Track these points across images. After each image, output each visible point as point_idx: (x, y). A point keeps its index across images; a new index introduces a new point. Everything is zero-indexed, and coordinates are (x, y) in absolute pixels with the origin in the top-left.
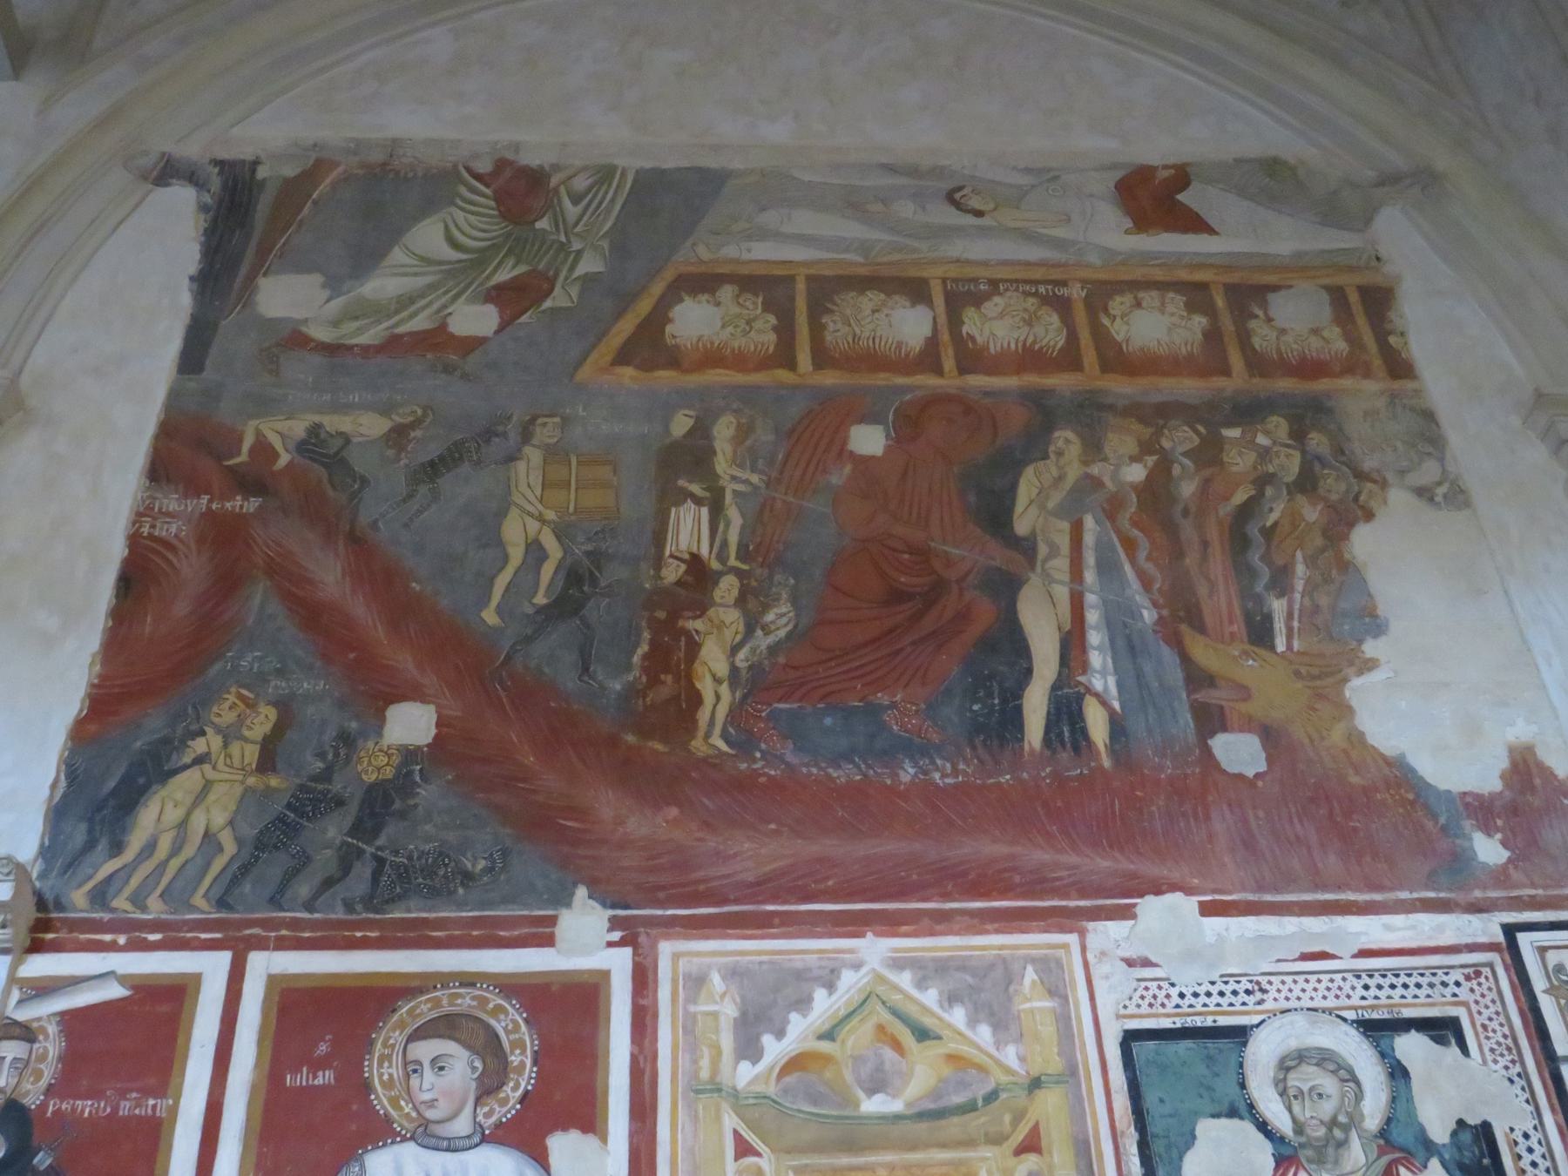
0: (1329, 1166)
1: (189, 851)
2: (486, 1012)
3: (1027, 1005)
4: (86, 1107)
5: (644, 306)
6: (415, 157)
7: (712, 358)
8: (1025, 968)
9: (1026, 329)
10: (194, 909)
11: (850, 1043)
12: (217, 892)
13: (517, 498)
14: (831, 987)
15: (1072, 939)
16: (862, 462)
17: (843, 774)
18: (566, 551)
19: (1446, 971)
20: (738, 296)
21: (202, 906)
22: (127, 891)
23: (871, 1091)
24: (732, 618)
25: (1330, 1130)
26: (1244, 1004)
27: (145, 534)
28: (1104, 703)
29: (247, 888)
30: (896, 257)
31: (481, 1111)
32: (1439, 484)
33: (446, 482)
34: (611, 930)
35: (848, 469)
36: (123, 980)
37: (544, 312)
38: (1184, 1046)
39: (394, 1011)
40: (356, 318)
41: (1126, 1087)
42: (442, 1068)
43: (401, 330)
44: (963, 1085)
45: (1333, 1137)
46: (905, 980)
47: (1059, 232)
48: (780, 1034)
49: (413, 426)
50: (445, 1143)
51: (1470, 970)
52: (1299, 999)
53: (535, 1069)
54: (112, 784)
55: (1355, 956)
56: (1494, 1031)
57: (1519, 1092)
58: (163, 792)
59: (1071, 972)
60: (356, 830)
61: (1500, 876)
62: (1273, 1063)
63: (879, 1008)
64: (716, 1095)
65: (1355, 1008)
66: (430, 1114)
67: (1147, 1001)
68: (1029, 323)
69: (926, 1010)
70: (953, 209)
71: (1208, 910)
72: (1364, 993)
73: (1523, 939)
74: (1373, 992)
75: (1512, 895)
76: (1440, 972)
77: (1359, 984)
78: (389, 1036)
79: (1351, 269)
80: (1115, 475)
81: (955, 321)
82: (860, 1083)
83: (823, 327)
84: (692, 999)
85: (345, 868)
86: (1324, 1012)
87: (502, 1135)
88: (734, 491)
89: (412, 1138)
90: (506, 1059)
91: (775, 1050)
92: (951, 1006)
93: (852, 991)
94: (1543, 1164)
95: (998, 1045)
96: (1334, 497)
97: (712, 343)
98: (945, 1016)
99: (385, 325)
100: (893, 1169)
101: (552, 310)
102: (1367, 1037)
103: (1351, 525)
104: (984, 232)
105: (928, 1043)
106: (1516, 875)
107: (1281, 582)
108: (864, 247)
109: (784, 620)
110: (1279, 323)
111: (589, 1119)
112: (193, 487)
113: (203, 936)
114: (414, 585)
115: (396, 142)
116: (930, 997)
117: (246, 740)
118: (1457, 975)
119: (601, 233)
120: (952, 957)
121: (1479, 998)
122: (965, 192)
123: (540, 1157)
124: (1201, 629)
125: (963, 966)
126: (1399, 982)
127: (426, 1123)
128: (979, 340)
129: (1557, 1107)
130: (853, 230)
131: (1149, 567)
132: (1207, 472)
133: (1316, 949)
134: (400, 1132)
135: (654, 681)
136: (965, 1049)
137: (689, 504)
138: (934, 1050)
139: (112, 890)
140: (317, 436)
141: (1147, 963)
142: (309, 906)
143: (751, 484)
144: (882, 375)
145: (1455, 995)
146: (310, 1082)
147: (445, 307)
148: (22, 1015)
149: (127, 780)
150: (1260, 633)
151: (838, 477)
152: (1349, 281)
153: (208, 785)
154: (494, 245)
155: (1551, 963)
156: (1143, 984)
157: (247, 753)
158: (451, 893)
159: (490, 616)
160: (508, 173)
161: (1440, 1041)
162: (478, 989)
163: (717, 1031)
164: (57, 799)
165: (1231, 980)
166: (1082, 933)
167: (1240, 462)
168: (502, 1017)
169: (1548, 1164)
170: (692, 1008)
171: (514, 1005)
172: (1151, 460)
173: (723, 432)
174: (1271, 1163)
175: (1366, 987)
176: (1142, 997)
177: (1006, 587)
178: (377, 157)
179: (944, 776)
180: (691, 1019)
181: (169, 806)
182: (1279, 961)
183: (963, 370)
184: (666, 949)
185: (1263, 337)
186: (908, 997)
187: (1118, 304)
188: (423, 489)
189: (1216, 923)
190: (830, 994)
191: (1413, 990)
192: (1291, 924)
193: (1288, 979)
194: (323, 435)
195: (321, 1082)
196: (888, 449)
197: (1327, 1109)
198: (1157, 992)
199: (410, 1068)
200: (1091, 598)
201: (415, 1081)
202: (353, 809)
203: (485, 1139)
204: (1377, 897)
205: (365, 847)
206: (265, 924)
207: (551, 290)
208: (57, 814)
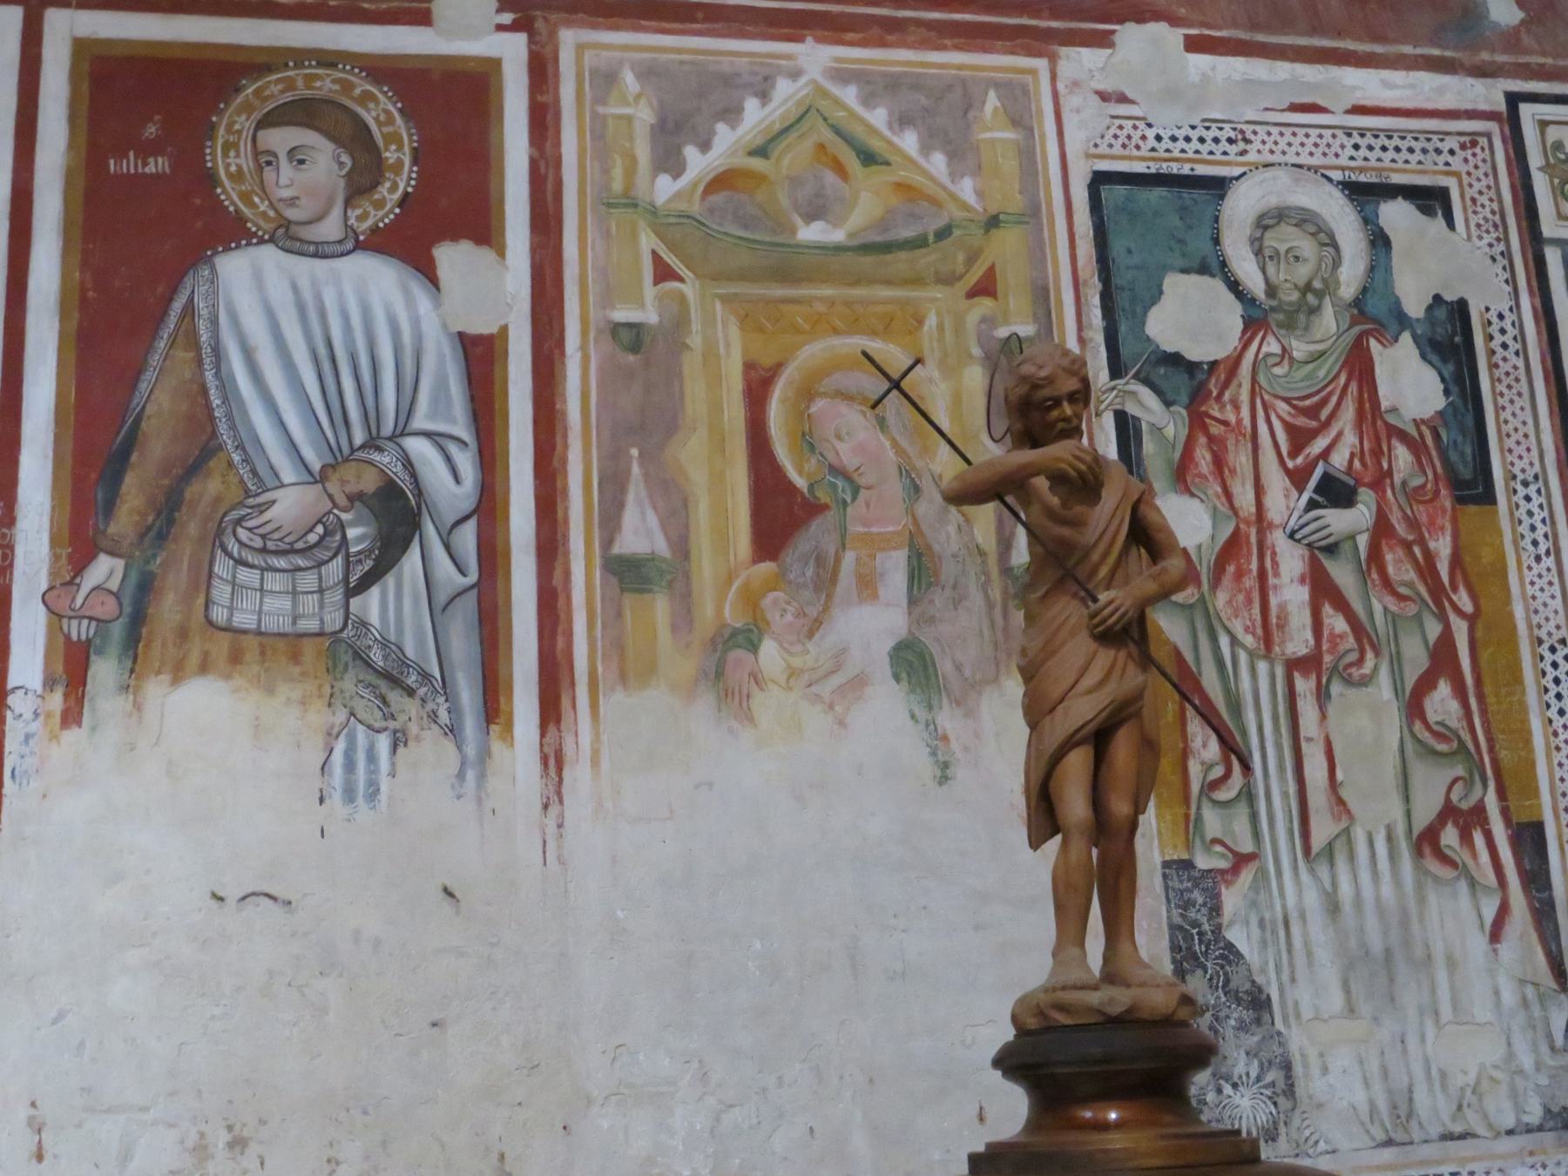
0: (1299, 332)
2: (353, 98)
3: (988, 135)
8: (987, 94)
11: (786, 162)
14: (764, 96)
15: (1041, 64)
19: (1441, 137)
23: (811, 217)
25: (1304, 295)
26: (1225, 153)
31: (353, 214)
34: (499, 11)
38: (1157, 194)
39: (238, 90)
41: (1091, 232)
42: (301, 162)
45: (1306, 303)
46: (849, 95)
48: (705, 146)
50: (312, 248)
51: (1466, 139)
52: (1284, 153)
53: (415, 169)
55: (1348, 112)
56: (1483, 206)
57: (1500, 271)
59: (1038, 102)
61: (1511, 39)
62: (1251, 218)
64: (630, 210)
65: (1343, 169)
66: (291, 214)
67: (1120, 141)
71: (1193, 45)
72: (1353, 153)
73: (1527, 111)
74: (1363, 152)
75: (1520, 61)
76: (1435, 137)
77: (1349, 143)
82: (796, 206)
84: (601, 100)
86: (1309, 169)
87: (378, 242)
89: (272, 240)
90: (380, 157)
91: (698, 164)
92: (901, 130)
93: (790, 104)
94: (1513, 346)
95: (954, 175)
98: (895, 139)
100: (833, 303)
102: (1352, 200)
105: (875, 168)
106: (1527, 40)
116: (878, 117)
120: (905, 73)
121: (1472, 170)
123: (428, 272)
125: (917, 84)
126: (1390, 144)
127: (287, 224)
129: (1536, 290)
134: (255, 233)
136: (918, 180)
138: (881, 177)
141: (1123, 99)
145: (1447, 164)
146: (140, 170)
155: (1550, 140)
156: (1117, 122)
161: (1427, 211)
162: (340, 71)
163: (631, 139)
165: (1214, 126)
166: (1053, 59)
168: (372, 105)
169: (1518, 346)
170: (601, 110)
171: (386, 93)
174: (1239, 325)
175: (1356, 147)
176: (1116, 137)
180: (600, 121)
182: (1267, 109)
184: (569, 39)
190: (764, 105)
191: (1405, 155)
192: (1283, 70)
193: (1275, 130)
195: (154, 170)
197: (1303, 272)
198: (1132, 132)
199: (263, 159)
201: (269, 174)
203: (359, 246)
204: (1378, 49)
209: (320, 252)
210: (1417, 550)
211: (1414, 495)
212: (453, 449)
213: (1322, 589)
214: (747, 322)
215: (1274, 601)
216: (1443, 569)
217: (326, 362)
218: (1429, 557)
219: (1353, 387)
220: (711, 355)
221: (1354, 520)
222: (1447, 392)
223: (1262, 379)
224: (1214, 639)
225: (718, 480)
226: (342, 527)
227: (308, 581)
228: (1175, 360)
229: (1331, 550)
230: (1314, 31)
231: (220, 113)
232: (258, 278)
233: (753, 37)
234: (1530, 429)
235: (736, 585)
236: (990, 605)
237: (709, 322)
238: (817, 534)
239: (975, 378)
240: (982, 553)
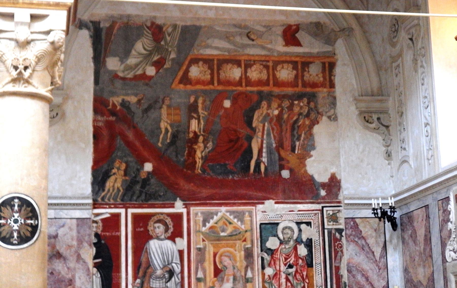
4: (108, 234)
5: (184, 67)
7: (198, 82)
9: (259, 74)
12: (121, 198)
13: (162, 117)
14: (217, 215)
15: (254, 208)
16: (226, 109)
17: (220, 177)
18: (172, 129)
21: (119, 201)
24: (202, 145)
28: (264, 164)
30: (235, 53)
32: (333, 115)
33: (149, 114)
35: (223, 111)
36: (110, 214)
38: (269, 226)
40: (127, 70)
44: (235, 231)
47: (269, 46)
48: (209, 223)
49: (142, 99)
54: (100, 179)
61: (323, 198)
66: (158, 235)
68: (260, 73)
69: (231, 219)
70: (247, 39)
71: (276, 203)
73: (325, 209)
74: (299, 217)
77: (297, 216)
78: (151, 223)
79: (328, 57)
80: (272, 113)
81: (246, 72)
84: (196, 217)
91: (208, 225)
95: (241, 225)
96: (313, 118)
103: (314, 125)
104: (254, 46)
106: (326, 198)
107: (299, 139)
108: (229, 50)
109: (211, 146)
110: (310, 73)
111: (181, 236)
112: (102, 115)
115: (129, 16)
116: (232, 217)
117: (121, 170)
118: (313, 215)
122: (251, 33)
123: (174, 241)
124: (283, 148)
128: (250, 77)
130: (226, 45)
131: (276, 135)
132: (289, 112)
133: (291, 210)
135: (189, 159)
136: (236, 225)
138: (231, 226)
139: (104, 198)
141: (265, 212)
142: (136, 201)
144: (230, 87)
147: (144, 67)
149: (103, 178)
150: (293, 150)
151: (221, 113)
152: (327, 60)
153: (116, 179)
158: (158, 199)
159: (160, 145)
160: (154, 27)
163: (199, 222)
166: (256, 207)
167: (296, 110)
170: (196, 219)
172: (280, 109)
173: (200, 101)
177: (250, 139)
178: (125, 20)
179: (236, 178)
180: (196, 220)
183: (246, 86)
185: (307, 77)
186: (228, 217)
187: (279, 68)
188: (145, 115)
189: (277, 205)
191: (305, 217)
192: (288, 206)
196: (231, 106)
197: (289, 236)
200: (265, 142)
201: (155, 230)
204: (303, 201)
206: (129, 204)
207: (165, 63)
208: (93, 184)
209: (162, 240)
210: (301, 274)
211: (301, 266)
212: (178, 265)
213: (287, 280)
214: (214, 247)
215: (281, 281)
216: (305, 277)
217: (163, 254)
218: (303, 275)
219: (294, 252)
220: (209, 251)
221: (293, 270)
222: (308, 252)
223: (281, 252)
224: (272, 286)
225: (210, 267)
226: (165, 275)
227: (161, 282)
228: (270, 249)
229: (289, 274)
230: (294, 199)
232: (154, 244)
233: (215, 207)
234: (320, 256)
235: (212, 281)
236: (243, 283)
237: (209, 247)
238: (222, 274)
239: (243, 253)
240: (242, 276)
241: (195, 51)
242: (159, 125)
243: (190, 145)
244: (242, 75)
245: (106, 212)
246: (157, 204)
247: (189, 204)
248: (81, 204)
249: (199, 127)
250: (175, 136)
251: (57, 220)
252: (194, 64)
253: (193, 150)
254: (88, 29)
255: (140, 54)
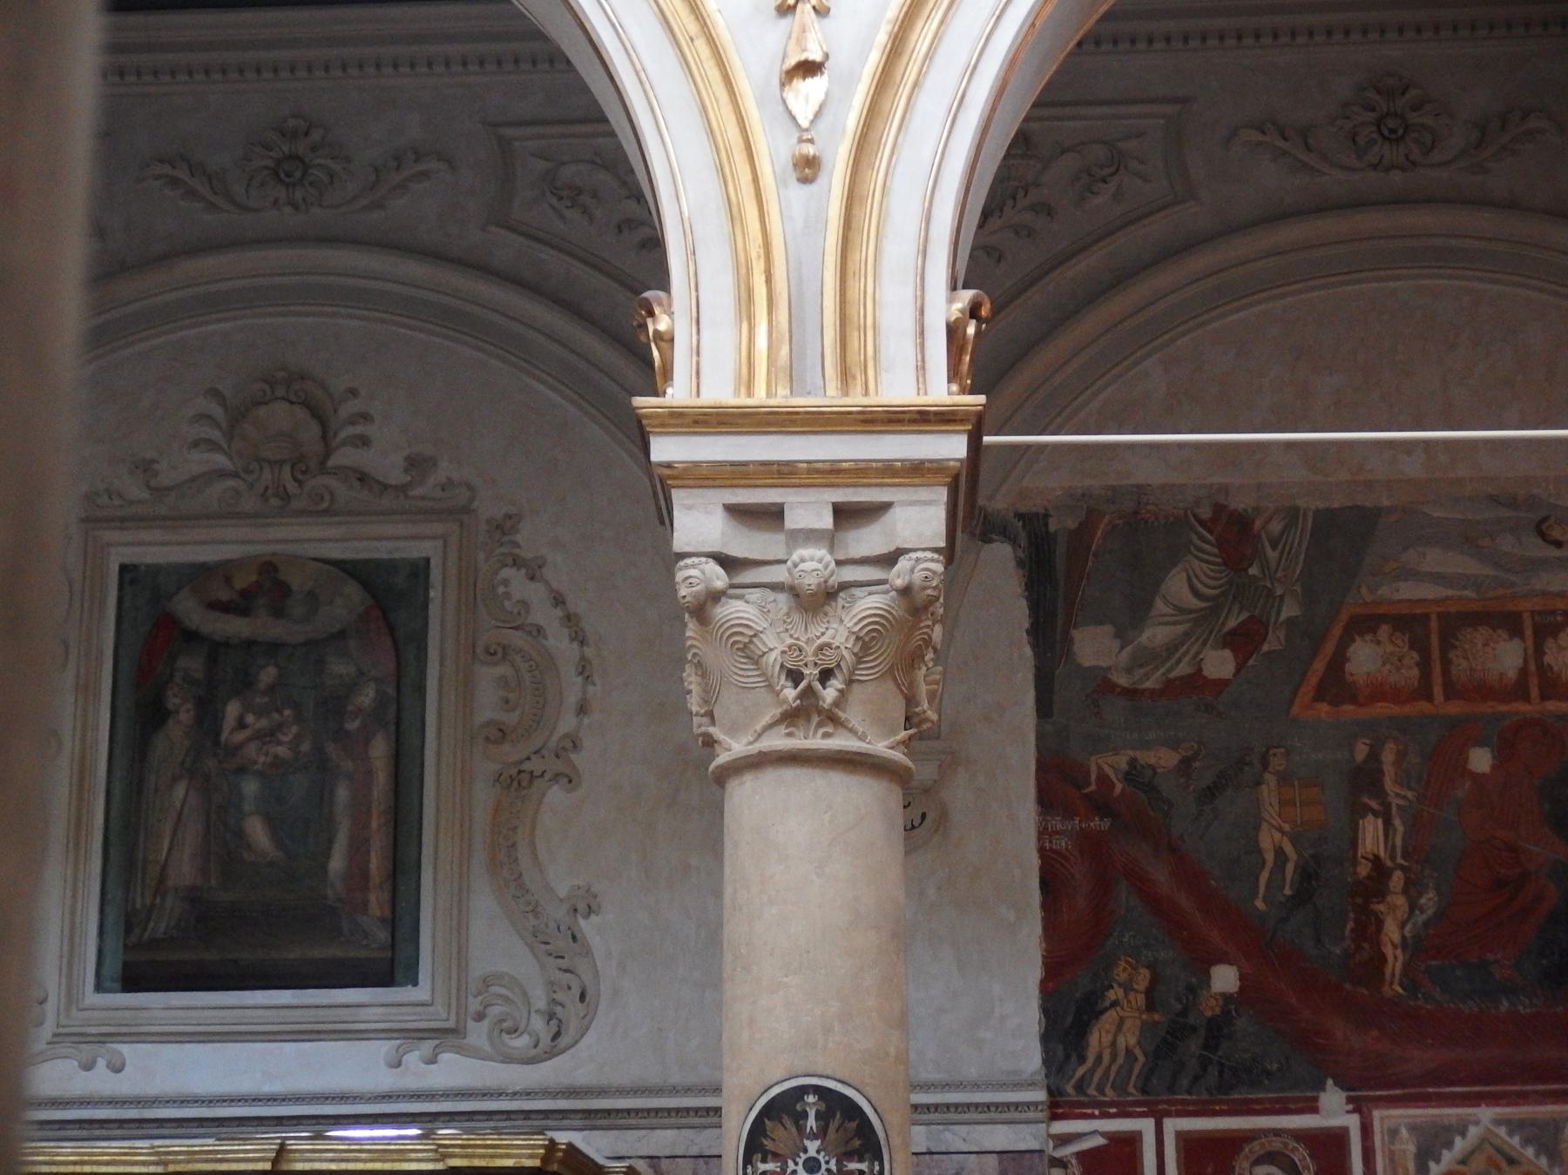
1: (1120, 1060)
5: (1329, 647)
6: (1157, 505)
7: (1379, 692)
10: (1132, 1094)
14: (1463, 1134)
16: (1477, 778)
20: (1392, 635)
22: (1093, 1085)
24: (1401, 901)
27: (1048, 848)
29: (1155, 1081)
30: (1501, 591)
34: (1347, 1104)
35: (1468, 784)
36: (1104, 1134)
37: (1264, 654)
40: (1141, 666)
43: (1173, 675)
46: (1502, 1131)
48: (1438, 1161)
54: (1070, 1019)
58: (1099, 1026)
60: (1206, 1047)
63: (1488, 1146)
69: (1513, 1148)
70: (1540, 541)
81: (1539, 651)
83: (1450, 662)
85: (1204, 1068)
88: (1397, 805)
95: (1551, 1166)
97: (1377, 679)
98: (1522, 1151)
99: (1162, 670)
101: (1270, 652)
112: (1069, 814)
113: (1138, 1109)
114: (1212, 882)
116: (1515, 1141)
119: (1296, 576)
122: (1552, 521)
128: (1556, 669)
137: (1370, 817)
140: (1135, 768)
142: (1189, 1093)
143: (1408, 799)
144: (1490, 703)
147: (1198, 653)
148: (1059, 1153)
151: (1462, 790)
153: (1122, 1020)
154: (1223, 593)
157: (1138, 999)
159: (1259, 904)
164: (1043, 1030)
170: (1393, 1148)
173: (1388, 756)
179: (1525, 1008)
180: (1392, 1153)
181: (1104, 1034)
183: (1544, 697)
184: (1377, 1114)
194: (1138, 767)
196: (1494, 767)
202: (1202, 1032)
205: (1212, 1056)
206: (1168, 1102)
207: (1267, 633)
208: (1046, 1038)
231: (1236, 1161)
241: (1364, 590)
242: (1257, 841)
243: (1359, 901)
244: (1526, 661)
245: (1092, 1130)
246: (1258, 1101)
247: (1368, 1098)
248: (992, 1104)
249: (1390, 843)
250: (1307, 875)
251: (935, 1156)
252: (1362, 634)
253: (1373, 919)
254: (1013, 540)
255: (1181, 610)
